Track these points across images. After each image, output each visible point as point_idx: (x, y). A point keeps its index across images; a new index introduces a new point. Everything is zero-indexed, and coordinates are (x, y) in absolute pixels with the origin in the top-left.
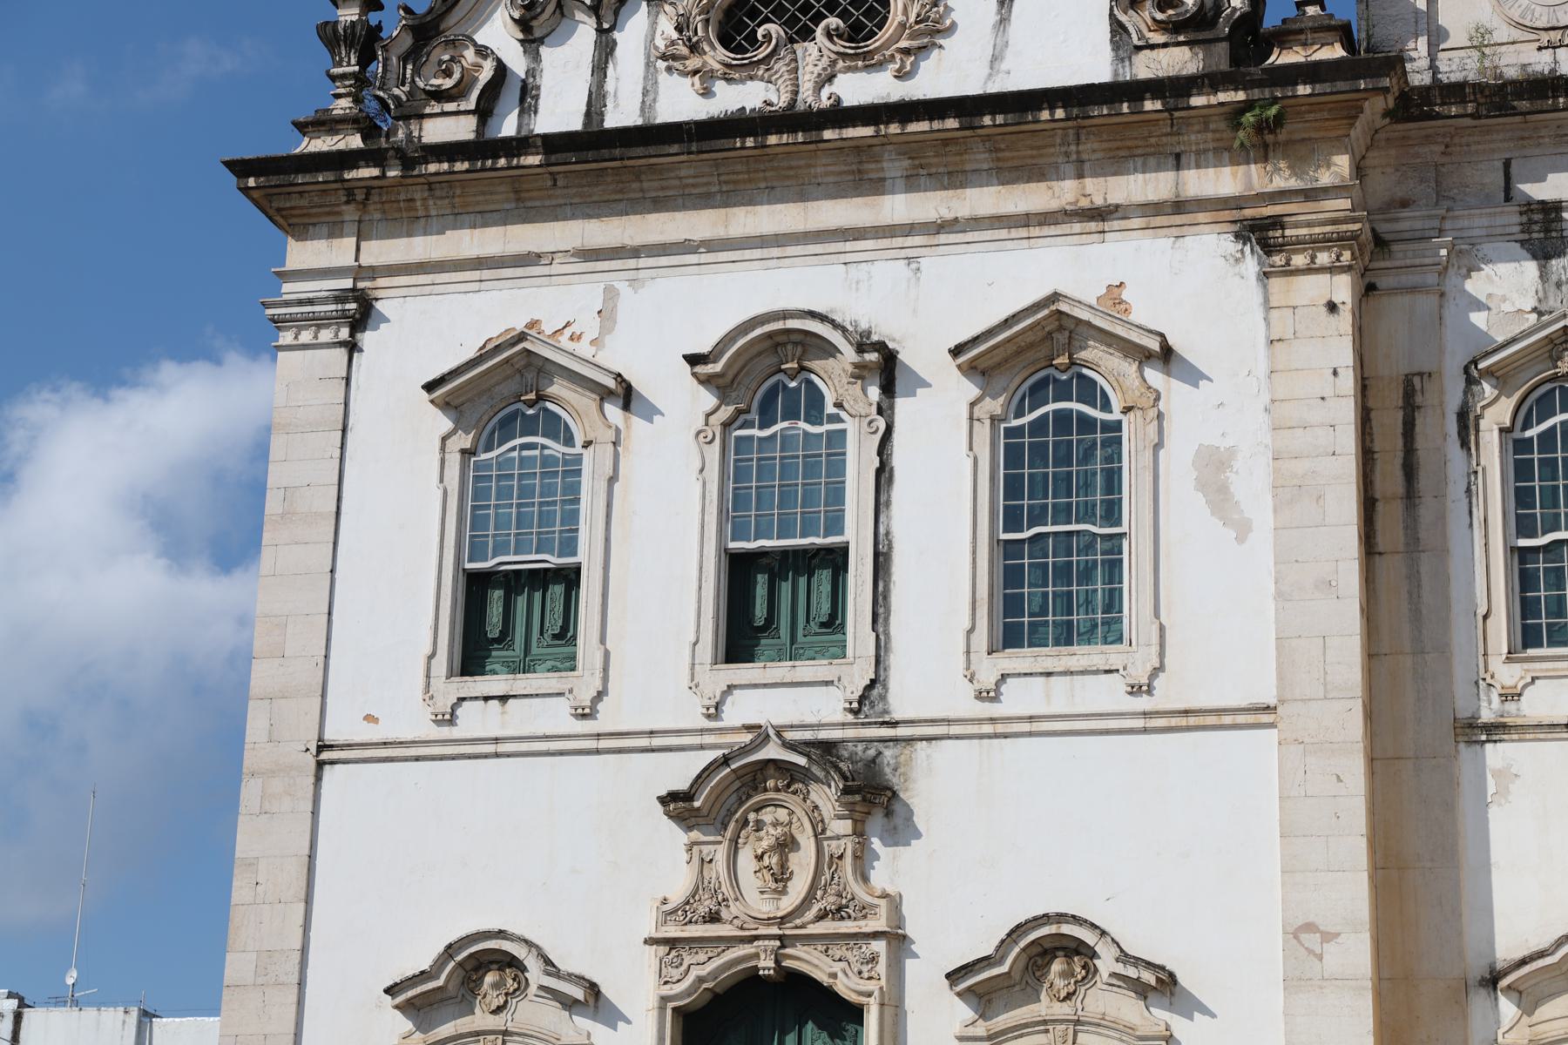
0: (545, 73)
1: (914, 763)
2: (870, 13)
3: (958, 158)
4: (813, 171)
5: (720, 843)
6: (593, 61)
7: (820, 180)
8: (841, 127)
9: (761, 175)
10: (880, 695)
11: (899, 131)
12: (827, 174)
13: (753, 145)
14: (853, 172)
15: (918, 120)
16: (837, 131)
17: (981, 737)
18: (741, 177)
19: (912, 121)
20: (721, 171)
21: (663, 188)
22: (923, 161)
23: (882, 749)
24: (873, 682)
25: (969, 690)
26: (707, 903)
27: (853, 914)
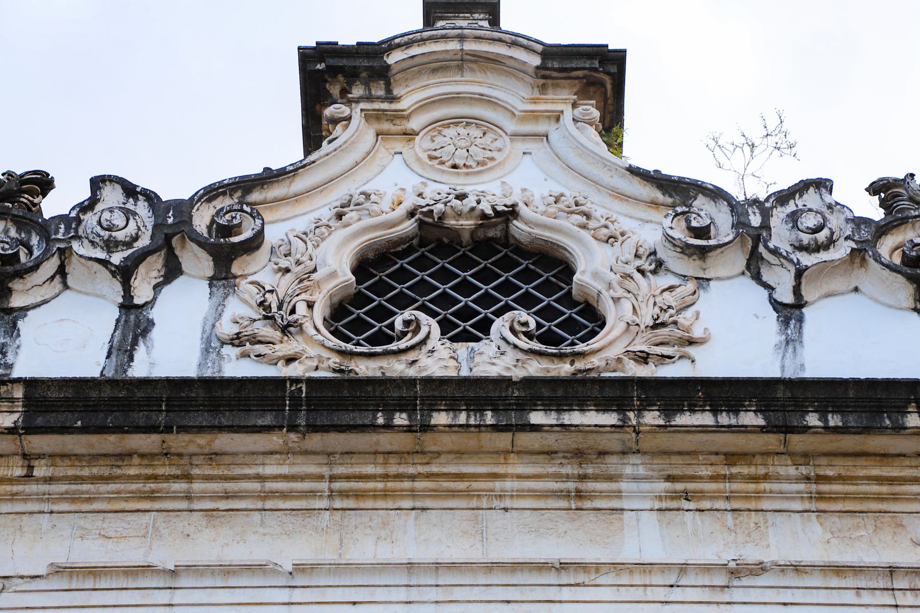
0: (22, 352)
2: (570, 326)
3: (752, 487)
4: (498, 485)
6: (111, 341)
7: (508, 503)
8: (559, 411)
9: (407, 485)
11: (662, 422)
12: (520, 494)
13: (406, 423)
14: (569, 492)
15: (692, 411)
16: (554, 415)
18: (371, 485)
19: (682, 411)
20: (340, 470)
21: (227, 496)
22: (691, 486)
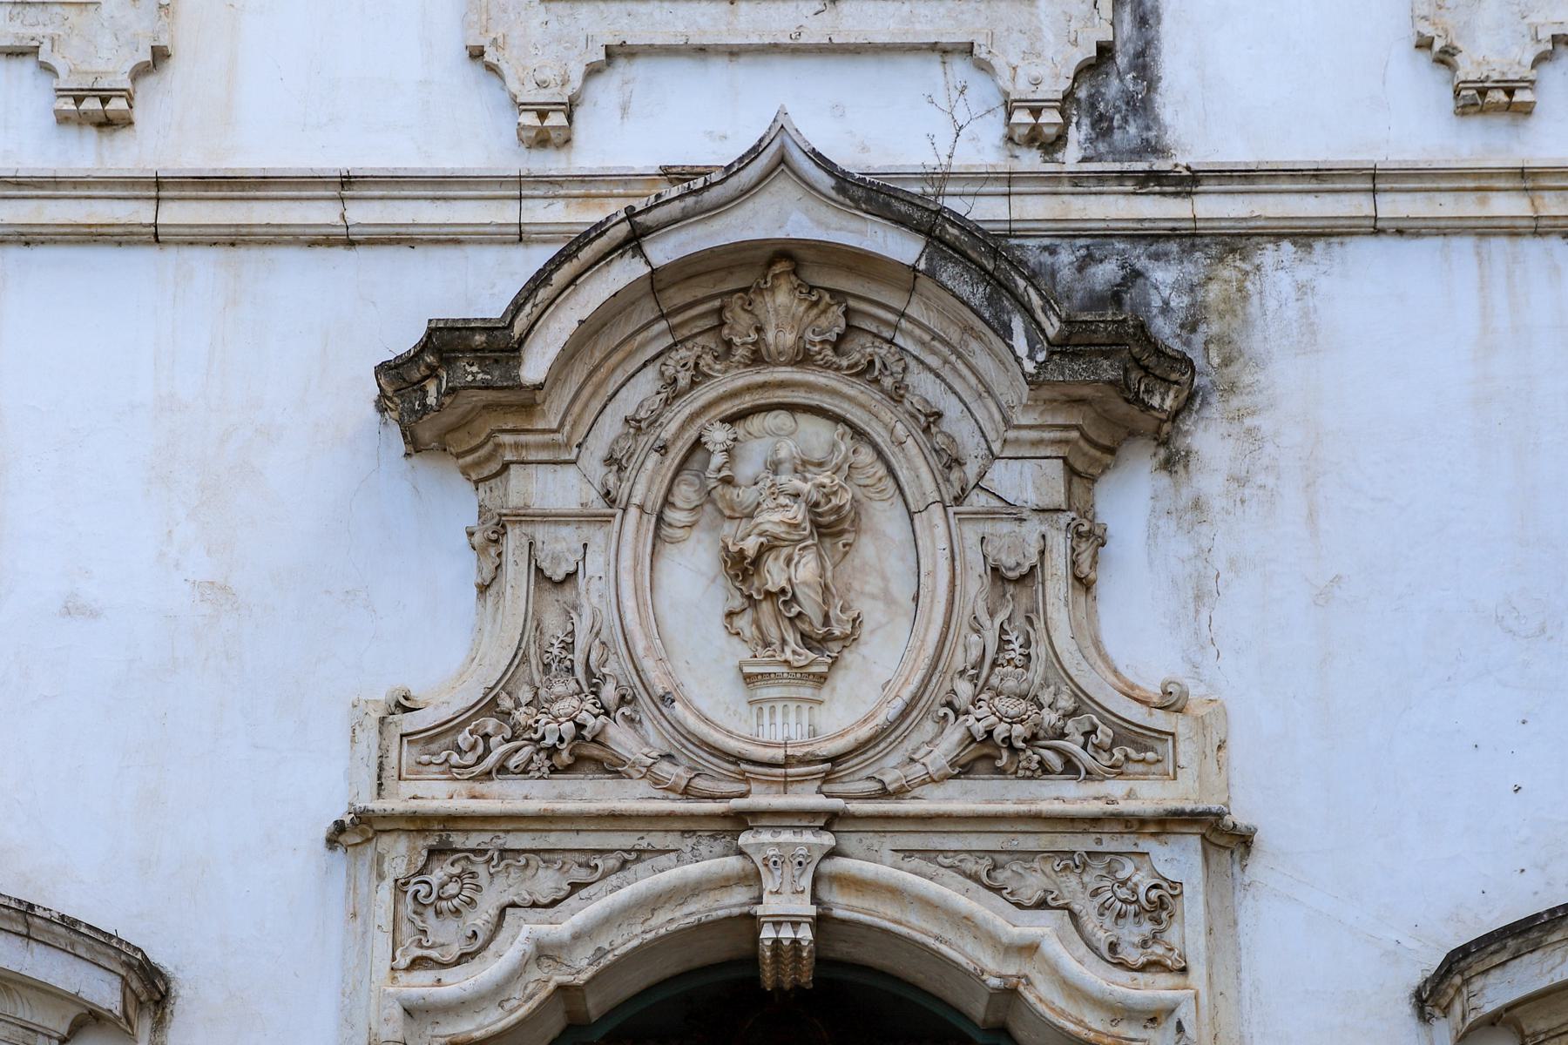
1: (1254, 308)
5: (605, 519)
10: (1130, 99)
17: (1485, 230)
23: (1142, 263)
24: (1105, 51)
25: (1435, 90)
26: (566, 706)
27: (1084, 758)
